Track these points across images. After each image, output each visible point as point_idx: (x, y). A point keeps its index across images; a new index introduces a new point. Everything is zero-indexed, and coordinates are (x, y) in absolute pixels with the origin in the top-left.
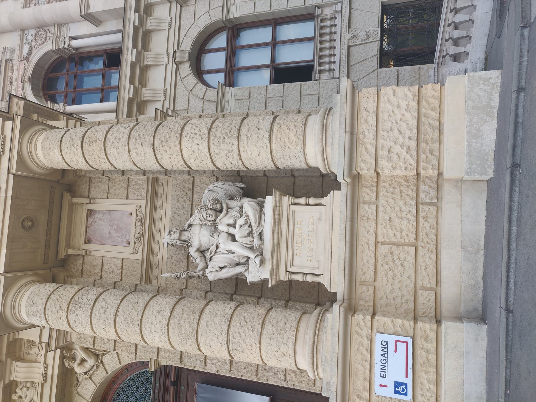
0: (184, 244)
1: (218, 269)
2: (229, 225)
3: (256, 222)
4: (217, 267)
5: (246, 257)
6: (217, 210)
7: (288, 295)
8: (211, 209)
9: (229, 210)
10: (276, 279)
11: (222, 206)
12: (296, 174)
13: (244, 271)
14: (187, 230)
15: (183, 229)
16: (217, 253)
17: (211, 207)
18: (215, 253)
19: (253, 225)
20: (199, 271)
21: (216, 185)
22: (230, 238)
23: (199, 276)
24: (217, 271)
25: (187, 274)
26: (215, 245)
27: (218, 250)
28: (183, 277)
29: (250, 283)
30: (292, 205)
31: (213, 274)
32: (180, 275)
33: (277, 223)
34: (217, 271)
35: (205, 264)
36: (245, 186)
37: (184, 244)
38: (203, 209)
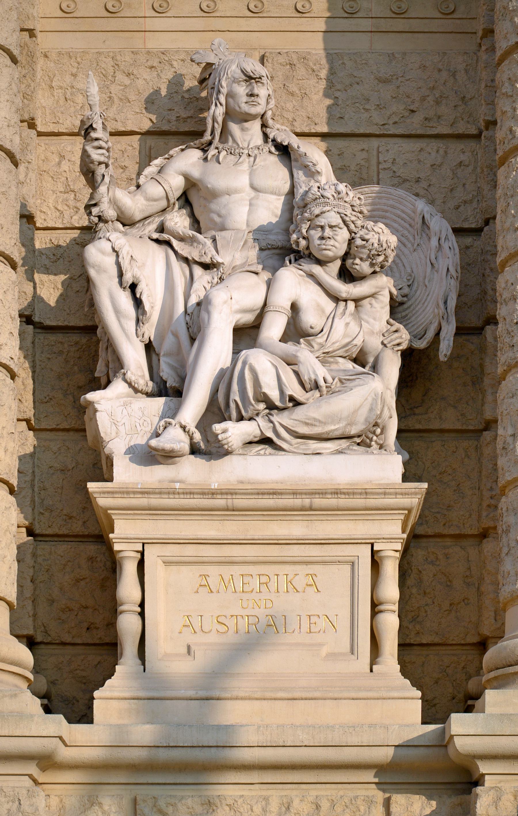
0: (213, 133)
1: (128, 278)
2: (294, 307)
3: (307, 424)
4: (138, 273)
5: (182, 379)
6: (349, 262)
7: (49, 531)
8: (351, 241)
9: (351, 305)
10: (113, 514)
11: (362, 278)
12: (488, 545)
13: (129, 375)
14: (266, 136)
15: (270, 122)
16: (185, 266)
17: (359, 242)
18: (186, 260)
19: (300, 412)
20: (114, 203)
21: (446, 246)
22: (249, 318)
23: (95, 205)
24: (121, 275)
25: (100, 163)
26: (219, 259)
27: (198, 271)
28: (89, 148)
29: (91, 404)
30: (373, 553)
31: (110, 261)
32: (97, 139)
33: (307, 502)
34: (121, 275)
35: (138, 216)
36: (442, 358)
37: (213, 133)
38: (349, 212)
